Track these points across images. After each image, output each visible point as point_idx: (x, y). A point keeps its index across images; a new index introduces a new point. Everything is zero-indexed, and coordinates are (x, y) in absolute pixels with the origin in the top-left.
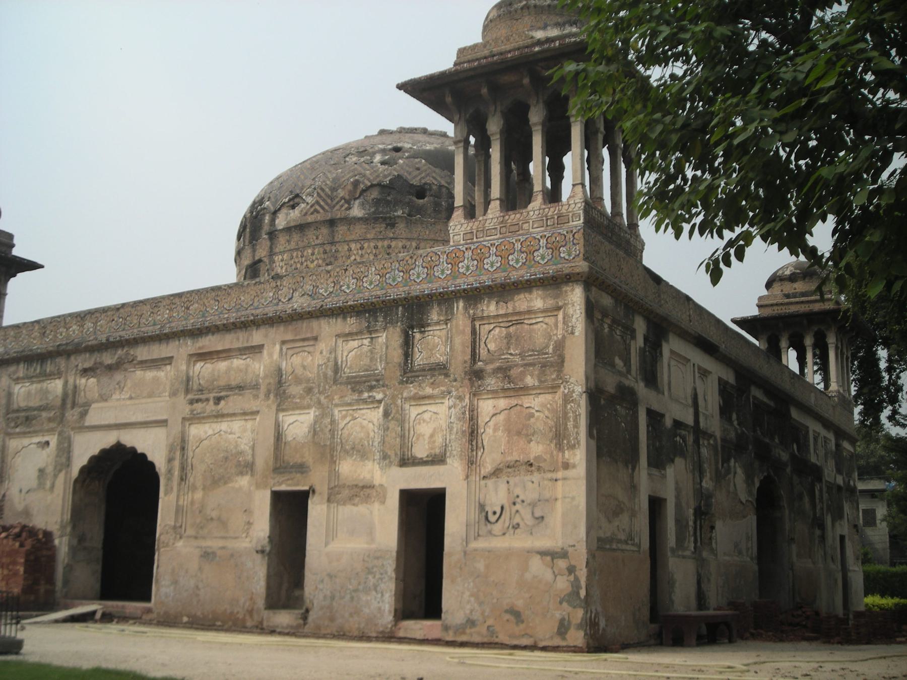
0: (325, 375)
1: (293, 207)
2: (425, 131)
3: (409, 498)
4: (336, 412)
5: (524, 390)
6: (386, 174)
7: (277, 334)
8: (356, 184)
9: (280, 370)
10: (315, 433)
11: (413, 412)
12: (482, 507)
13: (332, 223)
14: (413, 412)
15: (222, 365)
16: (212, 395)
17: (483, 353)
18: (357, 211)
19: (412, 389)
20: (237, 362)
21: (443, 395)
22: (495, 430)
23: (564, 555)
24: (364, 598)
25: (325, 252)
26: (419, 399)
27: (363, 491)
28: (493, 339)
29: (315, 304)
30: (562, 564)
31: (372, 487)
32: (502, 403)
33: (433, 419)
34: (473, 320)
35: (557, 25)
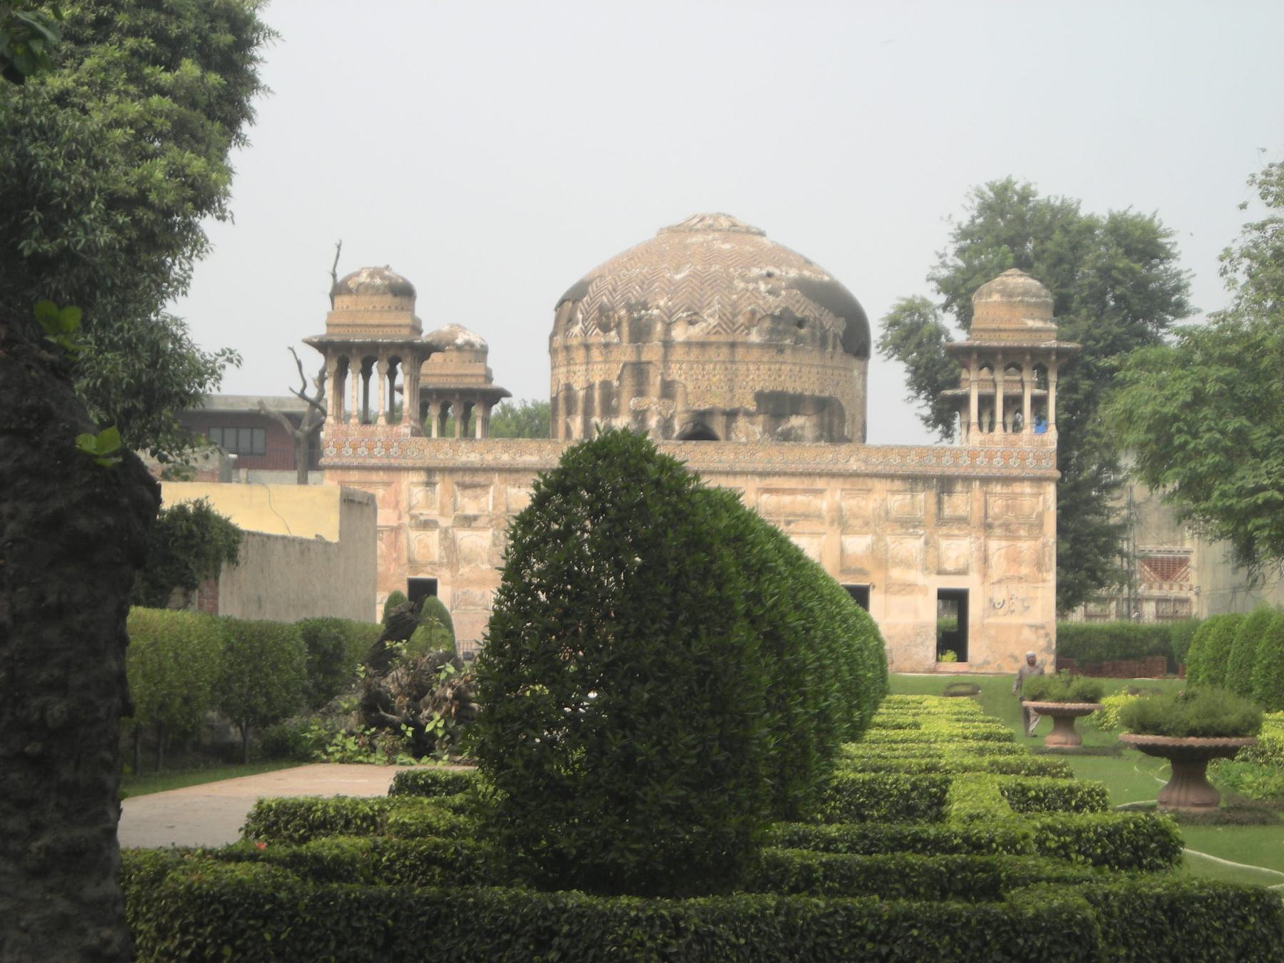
0: (879, 515)
1: (692, 323)
2: (748, 231)
3: (944, 595)
4: (889, 539)
5: (1019, 538)
6: (774, 304)
7: (837, 484)
8: (753, 313)
9: (840, 509)
10: (873, 551)
11: (944, 543)
12: (991, 600)
13: (733, 345)
14: (944, 543)
15: (786, 499)
16: (782, 519)
17: (991, 513)
18: (755, 337)
19: (944, 530)
20: (800, 498)
21: (966, 536)
22: (1000, 557)
23: (1043, 627)
24: (914, 650)
25: (726, 369)
26: (948, 536)
27: (908, 588)
28: (996, 506)
29: (871, 469)
30: (1042, 632)
31: (915, 585)
32: (1004, 543)
33: (958, 549)
34: (986, 493)
35: (1045, 320)
